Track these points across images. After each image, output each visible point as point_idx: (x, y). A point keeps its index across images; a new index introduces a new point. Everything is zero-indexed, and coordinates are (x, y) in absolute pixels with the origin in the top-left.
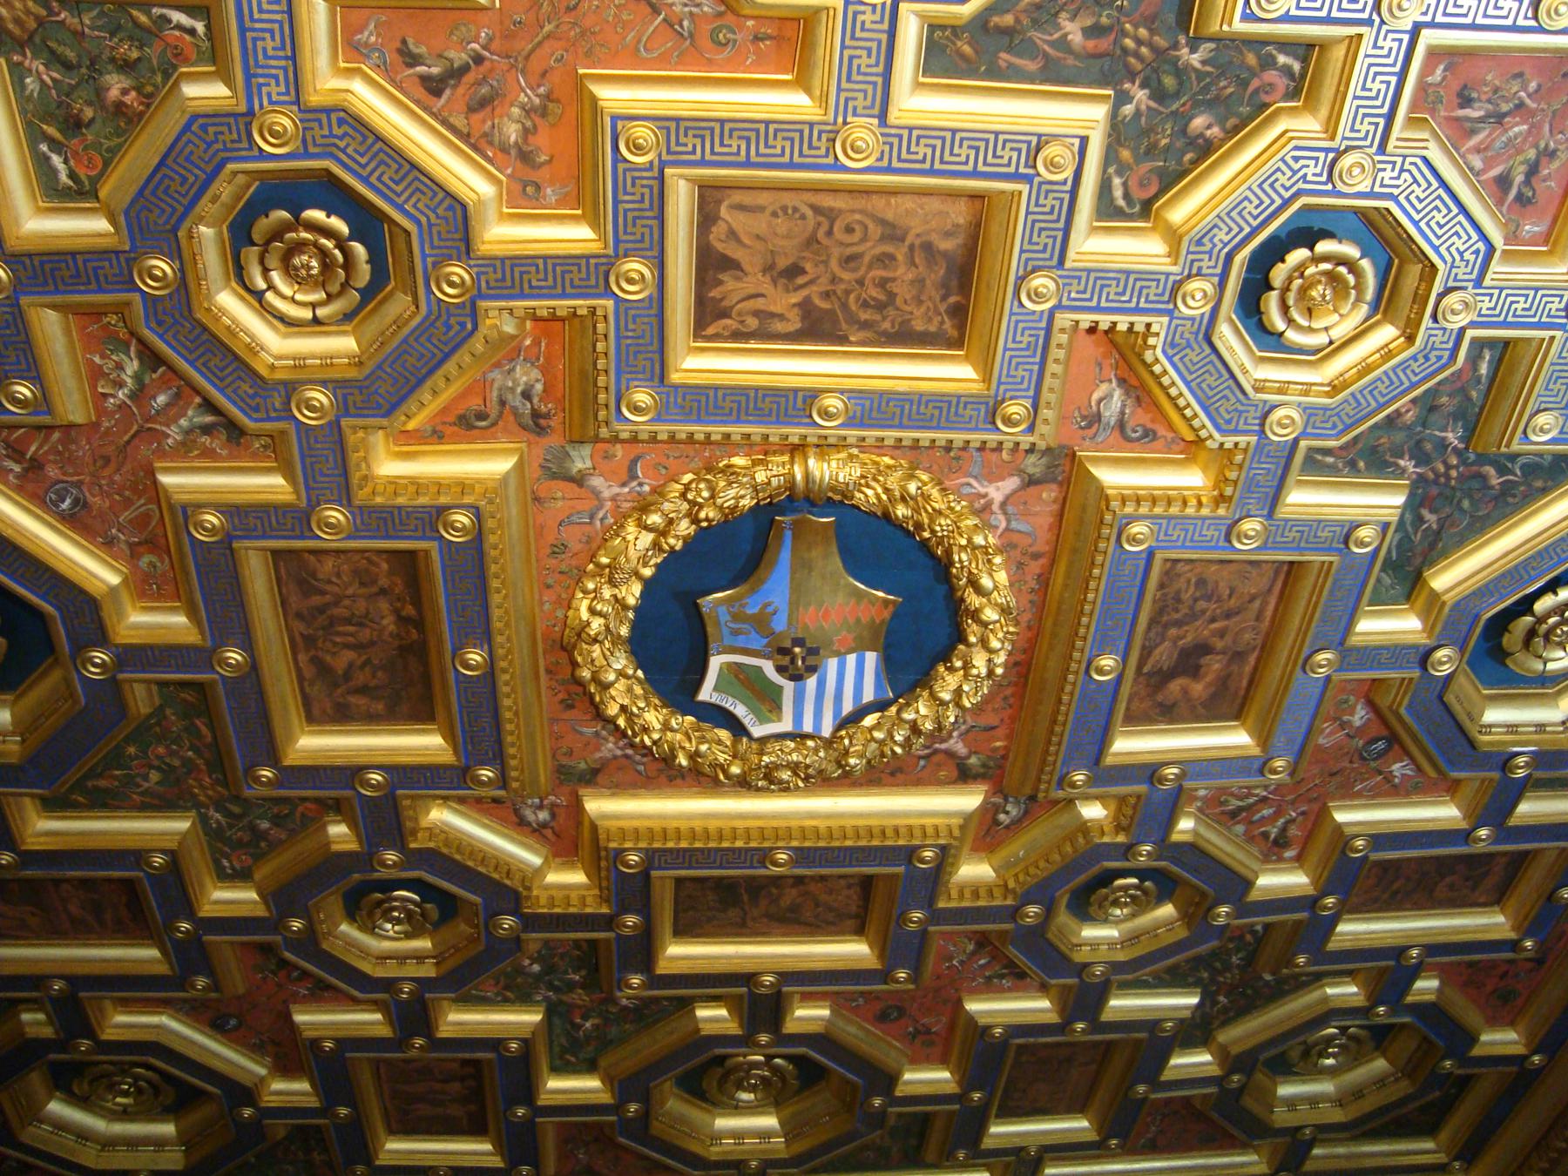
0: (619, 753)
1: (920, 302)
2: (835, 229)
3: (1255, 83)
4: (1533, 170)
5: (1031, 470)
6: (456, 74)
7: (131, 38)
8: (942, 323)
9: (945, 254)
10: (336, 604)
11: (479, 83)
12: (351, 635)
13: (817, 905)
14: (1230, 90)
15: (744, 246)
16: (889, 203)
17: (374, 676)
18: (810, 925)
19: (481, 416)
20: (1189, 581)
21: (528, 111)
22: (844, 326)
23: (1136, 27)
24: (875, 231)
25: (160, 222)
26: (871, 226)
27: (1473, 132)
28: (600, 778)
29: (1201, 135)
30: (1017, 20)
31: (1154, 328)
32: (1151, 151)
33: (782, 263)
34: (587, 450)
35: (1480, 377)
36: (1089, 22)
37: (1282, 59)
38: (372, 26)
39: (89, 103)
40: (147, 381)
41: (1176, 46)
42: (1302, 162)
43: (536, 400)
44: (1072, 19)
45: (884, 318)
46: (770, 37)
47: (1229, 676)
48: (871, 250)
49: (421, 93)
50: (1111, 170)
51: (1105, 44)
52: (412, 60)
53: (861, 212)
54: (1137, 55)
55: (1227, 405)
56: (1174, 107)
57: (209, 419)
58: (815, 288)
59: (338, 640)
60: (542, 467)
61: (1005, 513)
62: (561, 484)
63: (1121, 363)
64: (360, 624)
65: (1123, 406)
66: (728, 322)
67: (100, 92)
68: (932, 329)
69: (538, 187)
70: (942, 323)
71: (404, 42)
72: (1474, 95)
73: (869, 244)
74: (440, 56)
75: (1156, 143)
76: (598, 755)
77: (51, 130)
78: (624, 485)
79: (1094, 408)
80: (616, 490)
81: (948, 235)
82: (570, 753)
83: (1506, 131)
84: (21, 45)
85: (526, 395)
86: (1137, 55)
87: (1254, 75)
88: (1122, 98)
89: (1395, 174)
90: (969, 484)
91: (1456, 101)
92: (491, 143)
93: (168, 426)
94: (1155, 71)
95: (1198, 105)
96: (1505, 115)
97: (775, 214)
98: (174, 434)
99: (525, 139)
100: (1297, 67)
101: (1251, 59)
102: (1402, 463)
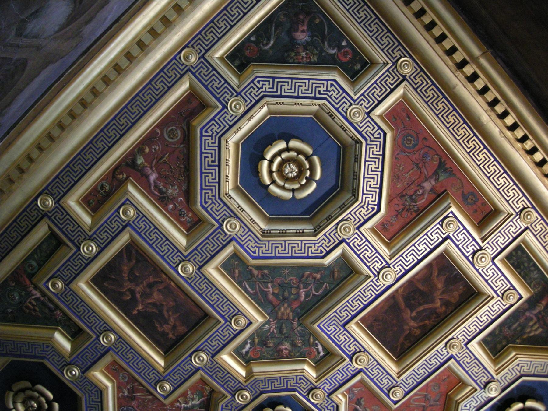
7: (303, 341)
25: (261, 387)
38: (359, 389)
39: (274, 343)
40: (195, 409)
52: (358, 403)
67: (280, 344)
71: (361, 398)
74: (365, 408)
77: (256, 340)
84: (277, 318)
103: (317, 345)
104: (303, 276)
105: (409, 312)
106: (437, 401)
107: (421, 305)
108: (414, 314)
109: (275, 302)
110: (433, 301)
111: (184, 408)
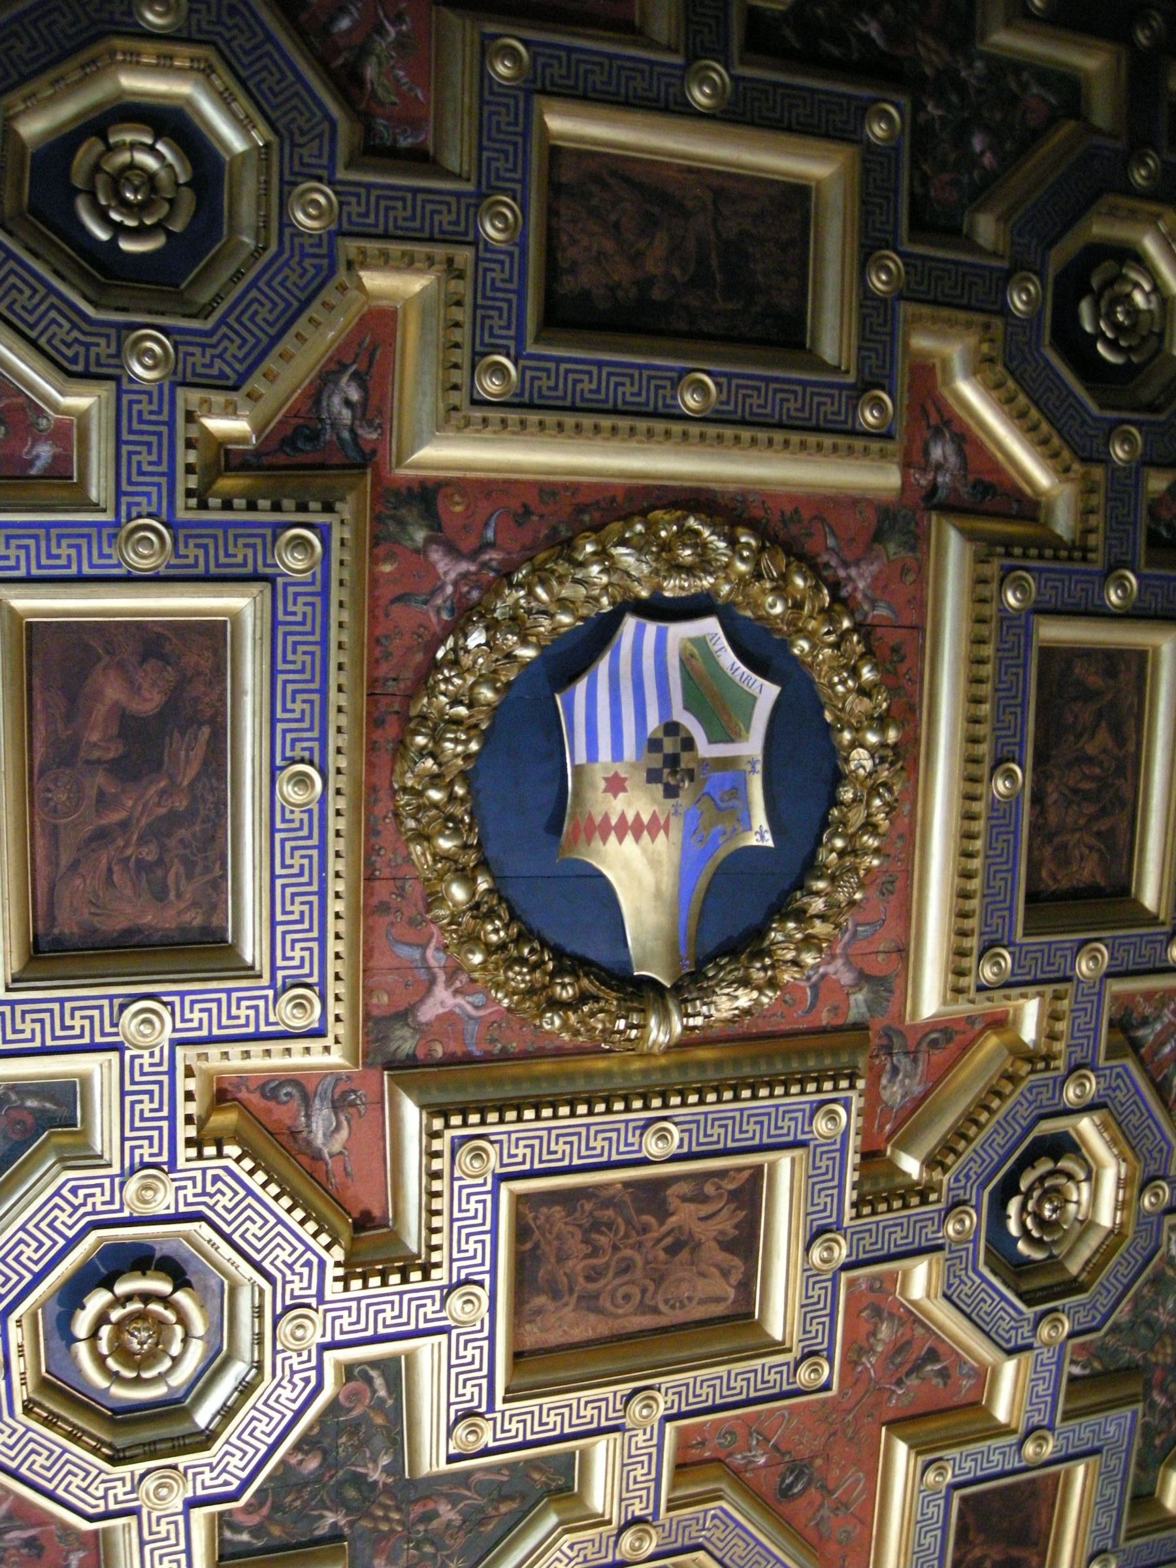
0: (853, 572)
2: (639, 1297)
3: (265, 1511)
5: (406, 1032)
6: (916, 1368)
8: (535, 1218)
9: (539, 1291)
10: (1092, 819)
11: (902, 1364)
12: (1085, 777)
13: (616, 225)
14: (289, 1499)
15: (717, 1266)
16: (594, 1329)
17: (1076, 717)
18: (626, 180)
19: (934, 1044)
20: (179, 896)
21: (871, 1350)
22: (627, 1199)
23: (392, 1531)
24: (605, 1302)
26: (608, 1305)
28: (871, 518)
29: (306, 1453)
30: (497, 1509)
31: (341, 1285)
32: (354, 1428)
33: (684, 1255)
34: (853, 1016)
36: (435, 1524)
37: (245, 1537)
41: (351, 1524)
42: (220, 1481)
43: (888, 1067)
44: (450, 1521)
45: (591, 1212)
46: (692, 1447)
47: (69, 717)
48: (607, 1282)
49: (941, 1349)
50: (390, 1402)
51: (417, 1510)
52: (944, 1374)
53: (617, 1317)
54: (386, 1508)
55: (224, 1201)
56: (341, 1473)
57: (1140, 1033)
59: (1097, 771)
60: (891, 991)
61: (429, 968)
62: (876, 972)
63: (323, 1180)
64: (1075, 791)
65: (308, 1125)
66: (731, 1187)
68: (544, 1210)
69: (871, 1288)
71: (945, 1384)
73: (609, 1287)
76: (875, 568)
78: (824, 976)
79: (343, 1118)
80: (830, 969)
81: (539, 1311)
82: (904, 571)
85: (895, 1070)
86: (386, 1508)
87: (268, 1518)
88: (394, 1469)
89: (111, 1493)
90: (477, 1007)
92: (900, 1318)
94: (365, 1499)
95: (317, 1478)
97: (690, 1299)
98: (1167, 1017)
99: (876, 1325)
100: (228, 1534)
101: (276, 1531)
103: (1084, 1367)
106: (817, 1524)
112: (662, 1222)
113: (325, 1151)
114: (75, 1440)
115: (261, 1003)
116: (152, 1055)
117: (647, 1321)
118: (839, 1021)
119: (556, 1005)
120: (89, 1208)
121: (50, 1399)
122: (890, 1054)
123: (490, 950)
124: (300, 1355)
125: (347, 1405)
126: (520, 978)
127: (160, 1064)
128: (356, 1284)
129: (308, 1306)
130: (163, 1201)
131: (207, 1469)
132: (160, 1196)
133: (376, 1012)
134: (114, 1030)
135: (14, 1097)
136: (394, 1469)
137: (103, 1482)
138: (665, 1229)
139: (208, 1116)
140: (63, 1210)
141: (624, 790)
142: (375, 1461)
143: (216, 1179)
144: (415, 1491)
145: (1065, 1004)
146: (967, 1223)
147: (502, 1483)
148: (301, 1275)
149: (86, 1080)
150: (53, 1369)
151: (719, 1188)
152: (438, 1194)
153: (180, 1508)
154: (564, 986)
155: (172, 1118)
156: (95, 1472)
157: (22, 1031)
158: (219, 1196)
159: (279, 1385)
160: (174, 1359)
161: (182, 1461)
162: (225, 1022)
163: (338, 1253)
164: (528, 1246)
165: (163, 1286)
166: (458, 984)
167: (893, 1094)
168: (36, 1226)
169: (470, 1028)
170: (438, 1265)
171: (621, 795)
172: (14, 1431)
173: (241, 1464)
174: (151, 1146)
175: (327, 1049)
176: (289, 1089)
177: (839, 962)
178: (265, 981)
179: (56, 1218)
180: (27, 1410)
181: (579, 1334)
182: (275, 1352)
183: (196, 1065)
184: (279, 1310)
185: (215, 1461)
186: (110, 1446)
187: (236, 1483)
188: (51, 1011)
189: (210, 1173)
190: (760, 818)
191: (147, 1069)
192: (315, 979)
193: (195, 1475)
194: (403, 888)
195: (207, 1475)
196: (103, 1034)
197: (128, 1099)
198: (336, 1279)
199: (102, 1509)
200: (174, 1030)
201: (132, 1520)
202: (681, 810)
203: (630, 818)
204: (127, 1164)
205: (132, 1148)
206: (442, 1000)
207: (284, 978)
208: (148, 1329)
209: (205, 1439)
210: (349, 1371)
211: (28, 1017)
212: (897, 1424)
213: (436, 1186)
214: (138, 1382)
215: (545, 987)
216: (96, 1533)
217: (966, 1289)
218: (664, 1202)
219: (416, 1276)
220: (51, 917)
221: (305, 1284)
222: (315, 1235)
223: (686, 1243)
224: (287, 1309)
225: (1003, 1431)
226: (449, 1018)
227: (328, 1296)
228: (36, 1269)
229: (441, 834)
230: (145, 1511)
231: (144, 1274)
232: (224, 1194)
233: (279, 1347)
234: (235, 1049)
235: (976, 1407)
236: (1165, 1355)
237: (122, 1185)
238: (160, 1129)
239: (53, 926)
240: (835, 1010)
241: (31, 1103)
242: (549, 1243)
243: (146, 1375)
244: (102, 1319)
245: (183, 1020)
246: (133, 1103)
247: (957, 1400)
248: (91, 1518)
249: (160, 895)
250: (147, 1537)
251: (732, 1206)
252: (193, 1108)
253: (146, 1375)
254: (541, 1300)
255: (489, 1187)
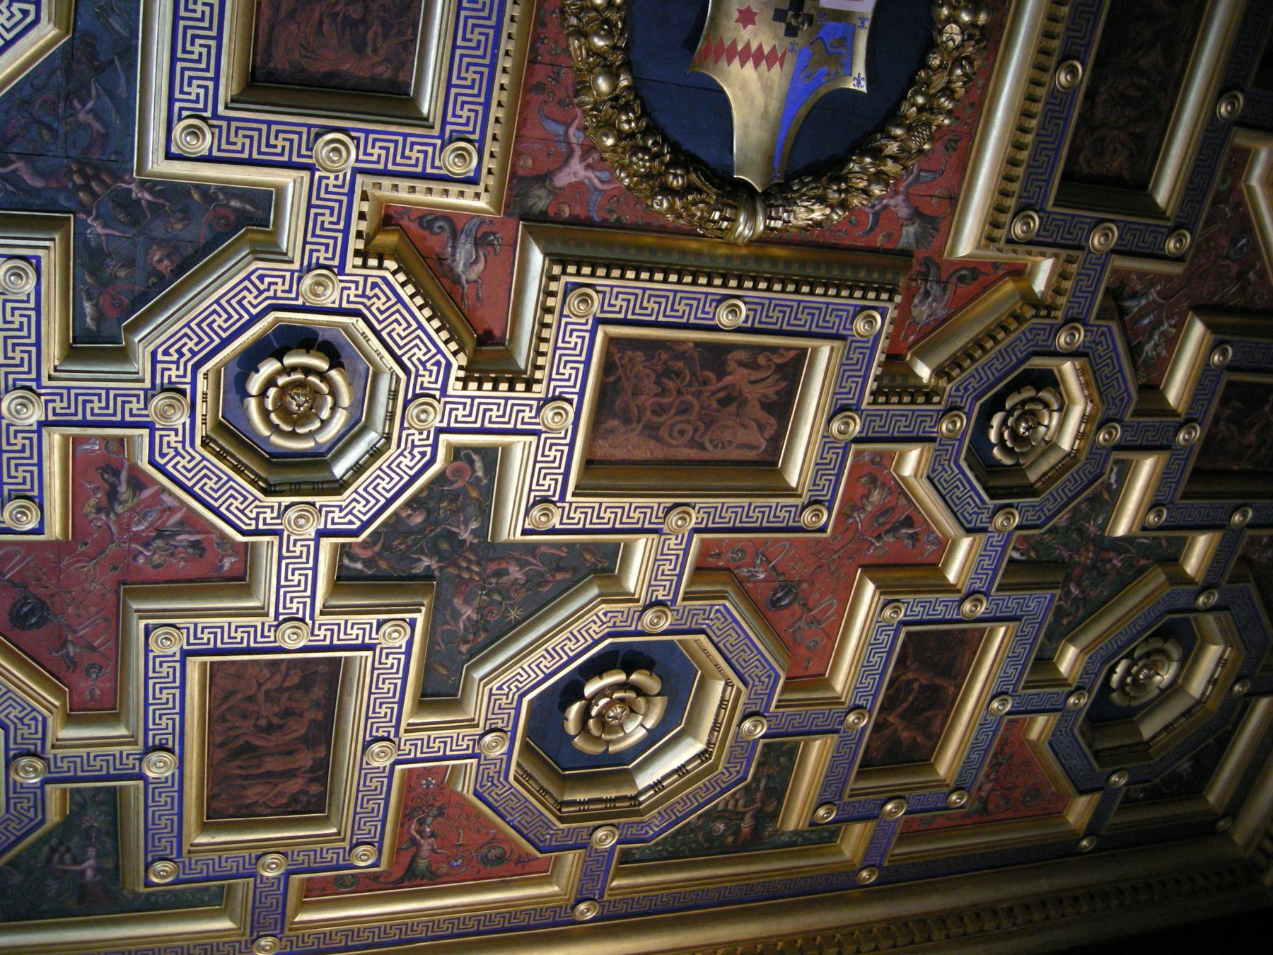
1: (636, 376)
3: (377, 548)
4: (113, 495)
5: (542, 192)
6: (894, 529)
8: (621, 358)
9: (614, 416)
14: (396, 542)
16: (651, 452)
19: (962, 279)
20: (375, 51)
21: (863, 508)
22: (696, 356)
23: (471, 579)
24: (664, 433)
26: (666, 435)
27: (181, 523)
30: (554, 576)
31: (460, 384)
33: (732, 408)
35: (90, 299)
36: (504, 579)
37: (359, 566)
41: (441, 569)
42: (346, 520)
43: (922, 290)
45: (665, 362)
46: (711, 556)
49: (916, 518)
50: (485, 481)
51: (493, 567)
52: (914, 538)
53: (670, 446)
54: (470, 561)
55: (379, 304)
57: (1128, 304)
58: (712, 388)
59: (1144, 82)
60: (937, 230)
61: (569, 143)
63: (458, 300)
65: (453, 255)
66: (779, 361)
68: (630, 353)
69: (872, 462)
70: (621, 358)
72: (190, 551)
73: (669, 422)
75: (450, 503)
77: (1106, 496)
78: (886, 207)
79: (481, 254)
80: (892, 202)
81: (611, 431)
83: (151, 525)
85: (927, 294)
86: (470, 561)
87: (379, 554)
88: (481, 533)
89: (262, 516)
90: (602, 182)
91: (205, 545)
93: (1154, 301)
95: (420, 530)
96: (157, 537)
97: (730, 443)
98: (1153, 295)
100: (346, 562)
102: (147, 196)
103: (1022, 554)
104: (1084, 606)
105: (924, 682)
107: (916, 699)
108: (916, 686)
109: (1104, 554)
110: (902, 716)
111: (1162, 324)
112: (719, 379)
113: (464, 278)
114: (240, 472)
115: (430, 149)
116: (336, 178)
117: (693, 454)
118: (891, 246)
119: (667, 190)
120: (271, 294)
121: (224, 439)
122: (926, 281)
123: (621, 135)
124: (421, 433)
125: (451, 478)
126: (641, 163)
127: (342, 186)
128: (473, 385)
129: (433, 397)
130: (330, 297)
131: (337, 510)
132: (329, 292)
133: (520, 172)
134: (309, 153)
135: (221, 196)
136: (481, 533)
137: (257, 507)
138: (721, 384)
139: (375, 235)
140: (251, 292)
141: (754, 23)
142: (466, 525)
143: (375, 285)
144: (494, 552)
145: (1074, 268)
146: (958, 425)
147: (561, 557)
148: (431, 372)
149: (281, 191)
150: (227, 416)
151: (769, 360)
152: (548, 326)
153: (313, 536)
154: (676, 176)
155: (346, 232)
156: (251, 498)
157: (235, 144)
158: (375, 300)
159: (401, 454)
160: (322, 421)
161: (319, 500)
162: (398, 159)
163: (462, 359)
164: (612, 379)
165: (324, 365)
166: (590, 160)
167: (922, 312)
168: (228, 302)
169: (594, 198)
170: (539, 381)
171: (750, 27)
172: (193, 458)
173: (364, 510)
174: (327, 251)
175: (477, 195)
176: (442, 224)
177: (900, 198)
178: (436, 132)
179: (244, 297)
180: (204, 444)
181: (639, 454)
182: (402, 428)
183: (371, 191)
184: (410, 396)
185: (344, 504)
186: (265, 481)
187: (358, 524)
188: (260, 131)
189: (370, 280)
190: (860, 68)
191: (331, 189)
192: (476, 137)
193: (327, 512)
194: (558, 74)
195: (337, 514)
196: (299, 155)
197: (313, 211)
198: (457, 379)
199: (253, 527)
200: (357, 160)
201: (276, 540)
202: (797, 48)
203: (754, 47)
204: (306, 263)
205: (312, 251)
206: (575, 172)
207: (452, 131)
208: (305, 396)
209: (339, 487)
210: (457, 453)
211: (241, 133)
212: (871, 569)
213: (548, 319)
214: (293, 435)
215: (660, 174)
216: (246, 543)
217: (946, 476)
218: (725, 363)
219: (520, 387)
220: (269, 55)
221: (433, 379)
222: (446, 342)
223: (735, 399)
224: (416, 396)
225: (951, 589)
226: (578, 187)
227: (450, 391)
228: (224, 335)
229: (598, 35)
230: (286, 533)
231: (308, 352)
232: (379, 299)
233: (406, 425)
234: (404, 184)
235: (935, 568)
236: (1087, 558)
237: (300, 279)
238: (336, 239)
239: (269, 61)
240: (889, 236)
241: (234, 203)
242: (628, 379)
243: (300, 431)
244: (271, 382)
245: (365, 154)
246: (316, 215)
247: (920, 560)
248: (244, 533)
249: (359, 47)
250: (285, 553)
251: (778, 377)
252: (363, 226)
253: (299, 431)
254: (614, 423)
255: (589, 327)
